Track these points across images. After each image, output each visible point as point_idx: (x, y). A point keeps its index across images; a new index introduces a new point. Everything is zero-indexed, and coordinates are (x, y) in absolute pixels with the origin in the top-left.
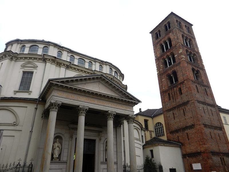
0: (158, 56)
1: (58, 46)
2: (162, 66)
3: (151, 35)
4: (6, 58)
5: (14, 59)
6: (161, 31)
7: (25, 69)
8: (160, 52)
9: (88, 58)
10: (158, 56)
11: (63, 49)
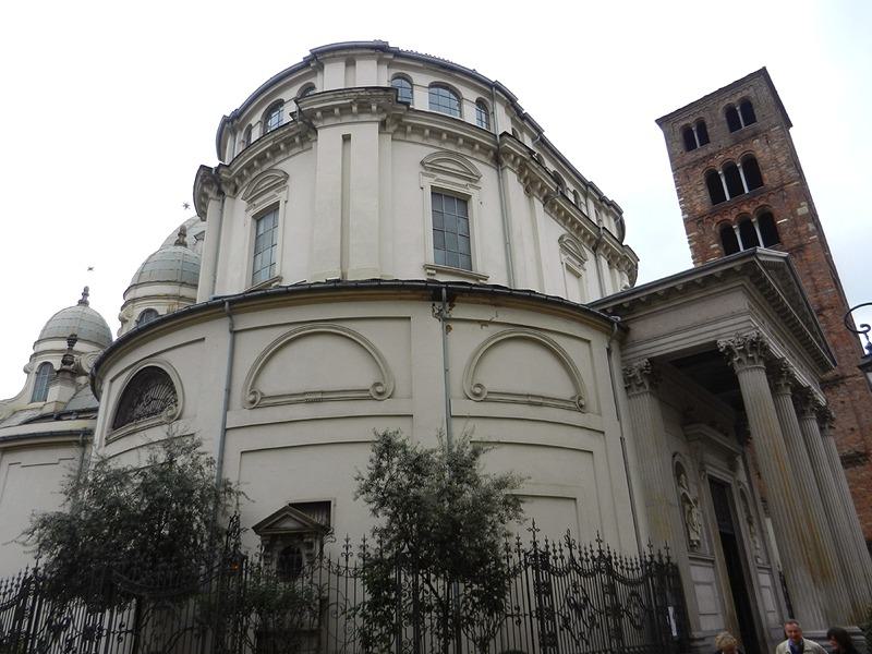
0: (699, 209)
1: (515, 107)
2: (717, 248)
3: (659, 134)
4: (364, 117)
5: (391, 129)
6: (708, 122)
7: (438, 180)
8: (702, 198)
9: (573, 177)
10: (699, 209)
11: (526, 123)
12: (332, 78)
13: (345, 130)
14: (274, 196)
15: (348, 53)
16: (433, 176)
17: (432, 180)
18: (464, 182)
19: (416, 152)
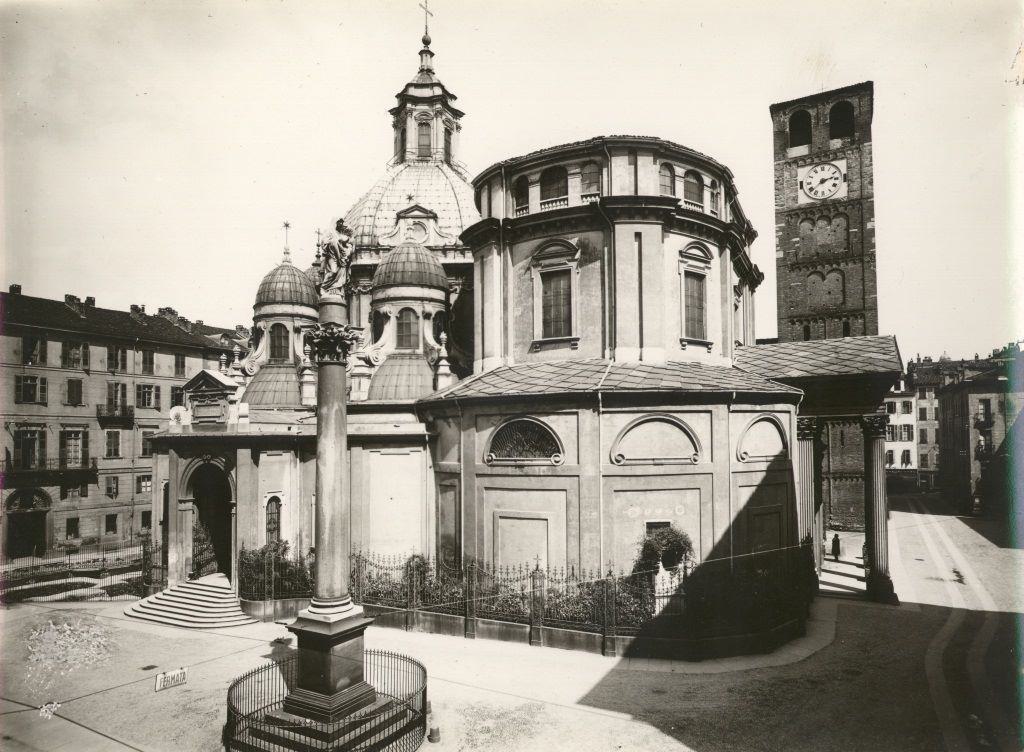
12: (621, 178)
13: (638, 228)
14: (565, 264)
15: (633, 147)
16: (686, 262)
17: (685, 266)
18: (702, 265)
19: (678, 241)
